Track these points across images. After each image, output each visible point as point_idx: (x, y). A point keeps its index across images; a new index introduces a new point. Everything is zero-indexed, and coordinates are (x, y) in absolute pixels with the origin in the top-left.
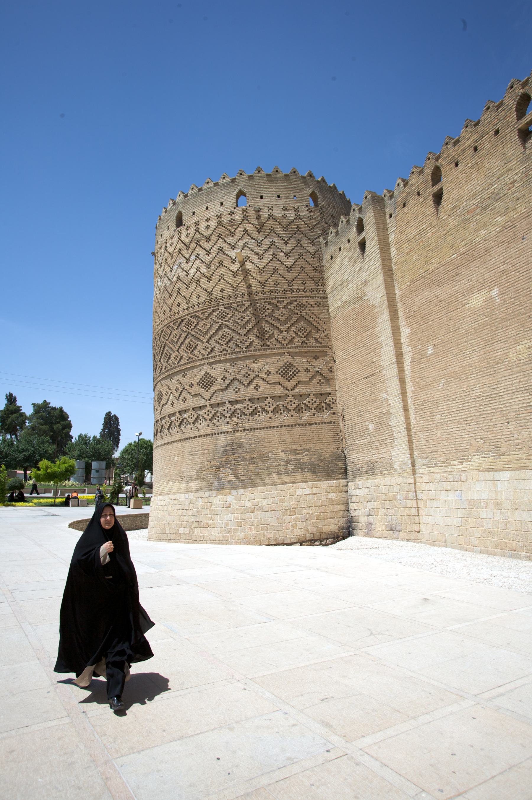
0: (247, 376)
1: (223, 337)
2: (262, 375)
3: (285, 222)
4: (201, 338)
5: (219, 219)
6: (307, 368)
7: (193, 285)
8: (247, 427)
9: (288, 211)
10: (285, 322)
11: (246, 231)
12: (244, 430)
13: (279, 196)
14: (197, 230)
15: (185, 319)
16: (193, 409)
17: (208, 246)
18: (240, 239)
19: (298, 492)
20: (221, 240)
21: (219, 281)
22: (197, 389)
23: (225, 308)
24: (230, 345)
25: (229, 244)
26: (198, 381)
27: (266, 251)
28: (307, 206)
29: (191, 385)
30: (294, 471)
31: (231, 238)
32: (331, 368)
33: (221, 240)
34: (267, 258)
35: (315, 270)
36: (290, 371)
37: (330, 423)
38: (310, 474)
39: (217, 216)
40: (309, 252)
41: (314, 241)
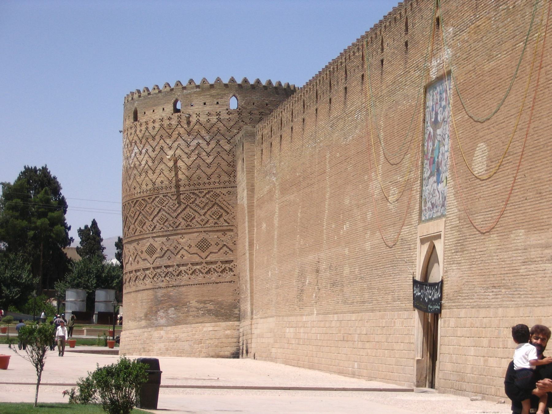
0: (176, 248)
1: (161, 219)
2: (186, 248)
3: (208, 126)
4: (148, 217)
5: (161, 122)
6: (217, 243)
7: (144, 175)
8: (175, 284)
9: (211, 116)
10: (203, 208)
11: (179, 134)
12: (173, 286)
13: (205, 104)
14: (147, 128)
15: (139, 200)
16: (143, 269)
17: (154, 144)
18: (175, 141)
19: (205, 329)
20: (162, 141)
21: (160, 175)
22: (145, 255)
23: (163, 196)
24: (166, 224)
25: (168, 144)
26: (146, 249)
27: (193, 151)
28: (227, 109)
29: (142, 252)
30: (203, 315)
31: (169, 140)
32: (235, 242)
33: (162, 141)
34: (194, 157)
35: (229, 165)
36: (205, 245)
37: (230, 282)
38: (213, 317)
39: (160, 119)
40: (225, 150)
41: (230, 140)
